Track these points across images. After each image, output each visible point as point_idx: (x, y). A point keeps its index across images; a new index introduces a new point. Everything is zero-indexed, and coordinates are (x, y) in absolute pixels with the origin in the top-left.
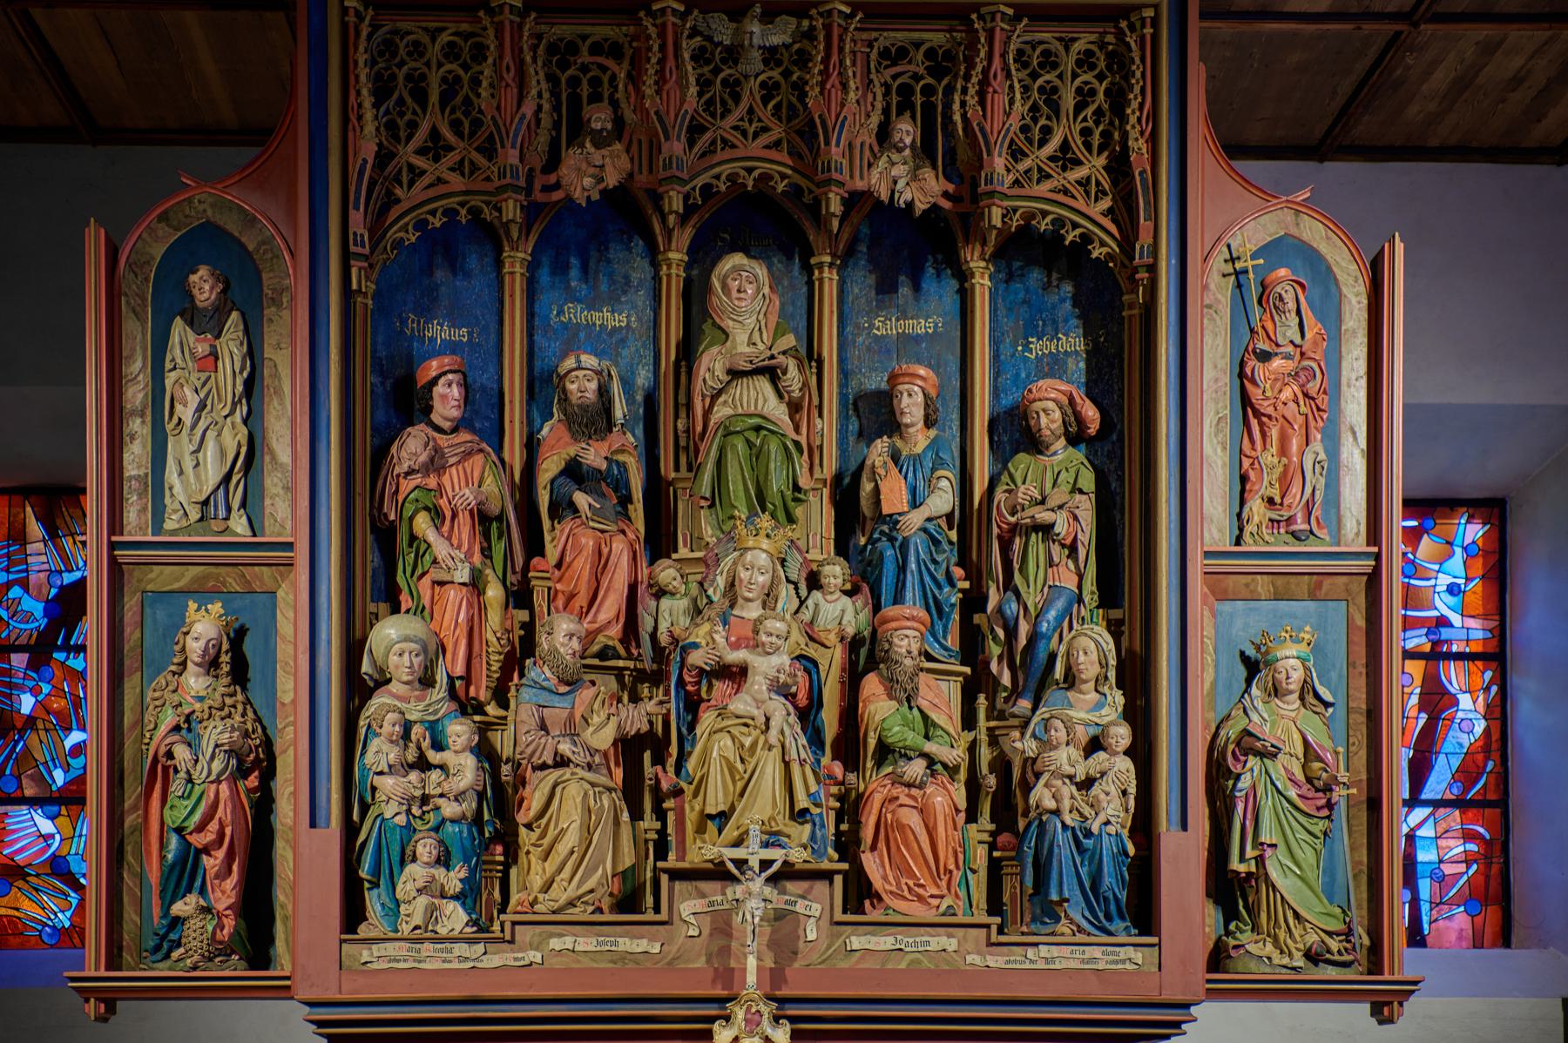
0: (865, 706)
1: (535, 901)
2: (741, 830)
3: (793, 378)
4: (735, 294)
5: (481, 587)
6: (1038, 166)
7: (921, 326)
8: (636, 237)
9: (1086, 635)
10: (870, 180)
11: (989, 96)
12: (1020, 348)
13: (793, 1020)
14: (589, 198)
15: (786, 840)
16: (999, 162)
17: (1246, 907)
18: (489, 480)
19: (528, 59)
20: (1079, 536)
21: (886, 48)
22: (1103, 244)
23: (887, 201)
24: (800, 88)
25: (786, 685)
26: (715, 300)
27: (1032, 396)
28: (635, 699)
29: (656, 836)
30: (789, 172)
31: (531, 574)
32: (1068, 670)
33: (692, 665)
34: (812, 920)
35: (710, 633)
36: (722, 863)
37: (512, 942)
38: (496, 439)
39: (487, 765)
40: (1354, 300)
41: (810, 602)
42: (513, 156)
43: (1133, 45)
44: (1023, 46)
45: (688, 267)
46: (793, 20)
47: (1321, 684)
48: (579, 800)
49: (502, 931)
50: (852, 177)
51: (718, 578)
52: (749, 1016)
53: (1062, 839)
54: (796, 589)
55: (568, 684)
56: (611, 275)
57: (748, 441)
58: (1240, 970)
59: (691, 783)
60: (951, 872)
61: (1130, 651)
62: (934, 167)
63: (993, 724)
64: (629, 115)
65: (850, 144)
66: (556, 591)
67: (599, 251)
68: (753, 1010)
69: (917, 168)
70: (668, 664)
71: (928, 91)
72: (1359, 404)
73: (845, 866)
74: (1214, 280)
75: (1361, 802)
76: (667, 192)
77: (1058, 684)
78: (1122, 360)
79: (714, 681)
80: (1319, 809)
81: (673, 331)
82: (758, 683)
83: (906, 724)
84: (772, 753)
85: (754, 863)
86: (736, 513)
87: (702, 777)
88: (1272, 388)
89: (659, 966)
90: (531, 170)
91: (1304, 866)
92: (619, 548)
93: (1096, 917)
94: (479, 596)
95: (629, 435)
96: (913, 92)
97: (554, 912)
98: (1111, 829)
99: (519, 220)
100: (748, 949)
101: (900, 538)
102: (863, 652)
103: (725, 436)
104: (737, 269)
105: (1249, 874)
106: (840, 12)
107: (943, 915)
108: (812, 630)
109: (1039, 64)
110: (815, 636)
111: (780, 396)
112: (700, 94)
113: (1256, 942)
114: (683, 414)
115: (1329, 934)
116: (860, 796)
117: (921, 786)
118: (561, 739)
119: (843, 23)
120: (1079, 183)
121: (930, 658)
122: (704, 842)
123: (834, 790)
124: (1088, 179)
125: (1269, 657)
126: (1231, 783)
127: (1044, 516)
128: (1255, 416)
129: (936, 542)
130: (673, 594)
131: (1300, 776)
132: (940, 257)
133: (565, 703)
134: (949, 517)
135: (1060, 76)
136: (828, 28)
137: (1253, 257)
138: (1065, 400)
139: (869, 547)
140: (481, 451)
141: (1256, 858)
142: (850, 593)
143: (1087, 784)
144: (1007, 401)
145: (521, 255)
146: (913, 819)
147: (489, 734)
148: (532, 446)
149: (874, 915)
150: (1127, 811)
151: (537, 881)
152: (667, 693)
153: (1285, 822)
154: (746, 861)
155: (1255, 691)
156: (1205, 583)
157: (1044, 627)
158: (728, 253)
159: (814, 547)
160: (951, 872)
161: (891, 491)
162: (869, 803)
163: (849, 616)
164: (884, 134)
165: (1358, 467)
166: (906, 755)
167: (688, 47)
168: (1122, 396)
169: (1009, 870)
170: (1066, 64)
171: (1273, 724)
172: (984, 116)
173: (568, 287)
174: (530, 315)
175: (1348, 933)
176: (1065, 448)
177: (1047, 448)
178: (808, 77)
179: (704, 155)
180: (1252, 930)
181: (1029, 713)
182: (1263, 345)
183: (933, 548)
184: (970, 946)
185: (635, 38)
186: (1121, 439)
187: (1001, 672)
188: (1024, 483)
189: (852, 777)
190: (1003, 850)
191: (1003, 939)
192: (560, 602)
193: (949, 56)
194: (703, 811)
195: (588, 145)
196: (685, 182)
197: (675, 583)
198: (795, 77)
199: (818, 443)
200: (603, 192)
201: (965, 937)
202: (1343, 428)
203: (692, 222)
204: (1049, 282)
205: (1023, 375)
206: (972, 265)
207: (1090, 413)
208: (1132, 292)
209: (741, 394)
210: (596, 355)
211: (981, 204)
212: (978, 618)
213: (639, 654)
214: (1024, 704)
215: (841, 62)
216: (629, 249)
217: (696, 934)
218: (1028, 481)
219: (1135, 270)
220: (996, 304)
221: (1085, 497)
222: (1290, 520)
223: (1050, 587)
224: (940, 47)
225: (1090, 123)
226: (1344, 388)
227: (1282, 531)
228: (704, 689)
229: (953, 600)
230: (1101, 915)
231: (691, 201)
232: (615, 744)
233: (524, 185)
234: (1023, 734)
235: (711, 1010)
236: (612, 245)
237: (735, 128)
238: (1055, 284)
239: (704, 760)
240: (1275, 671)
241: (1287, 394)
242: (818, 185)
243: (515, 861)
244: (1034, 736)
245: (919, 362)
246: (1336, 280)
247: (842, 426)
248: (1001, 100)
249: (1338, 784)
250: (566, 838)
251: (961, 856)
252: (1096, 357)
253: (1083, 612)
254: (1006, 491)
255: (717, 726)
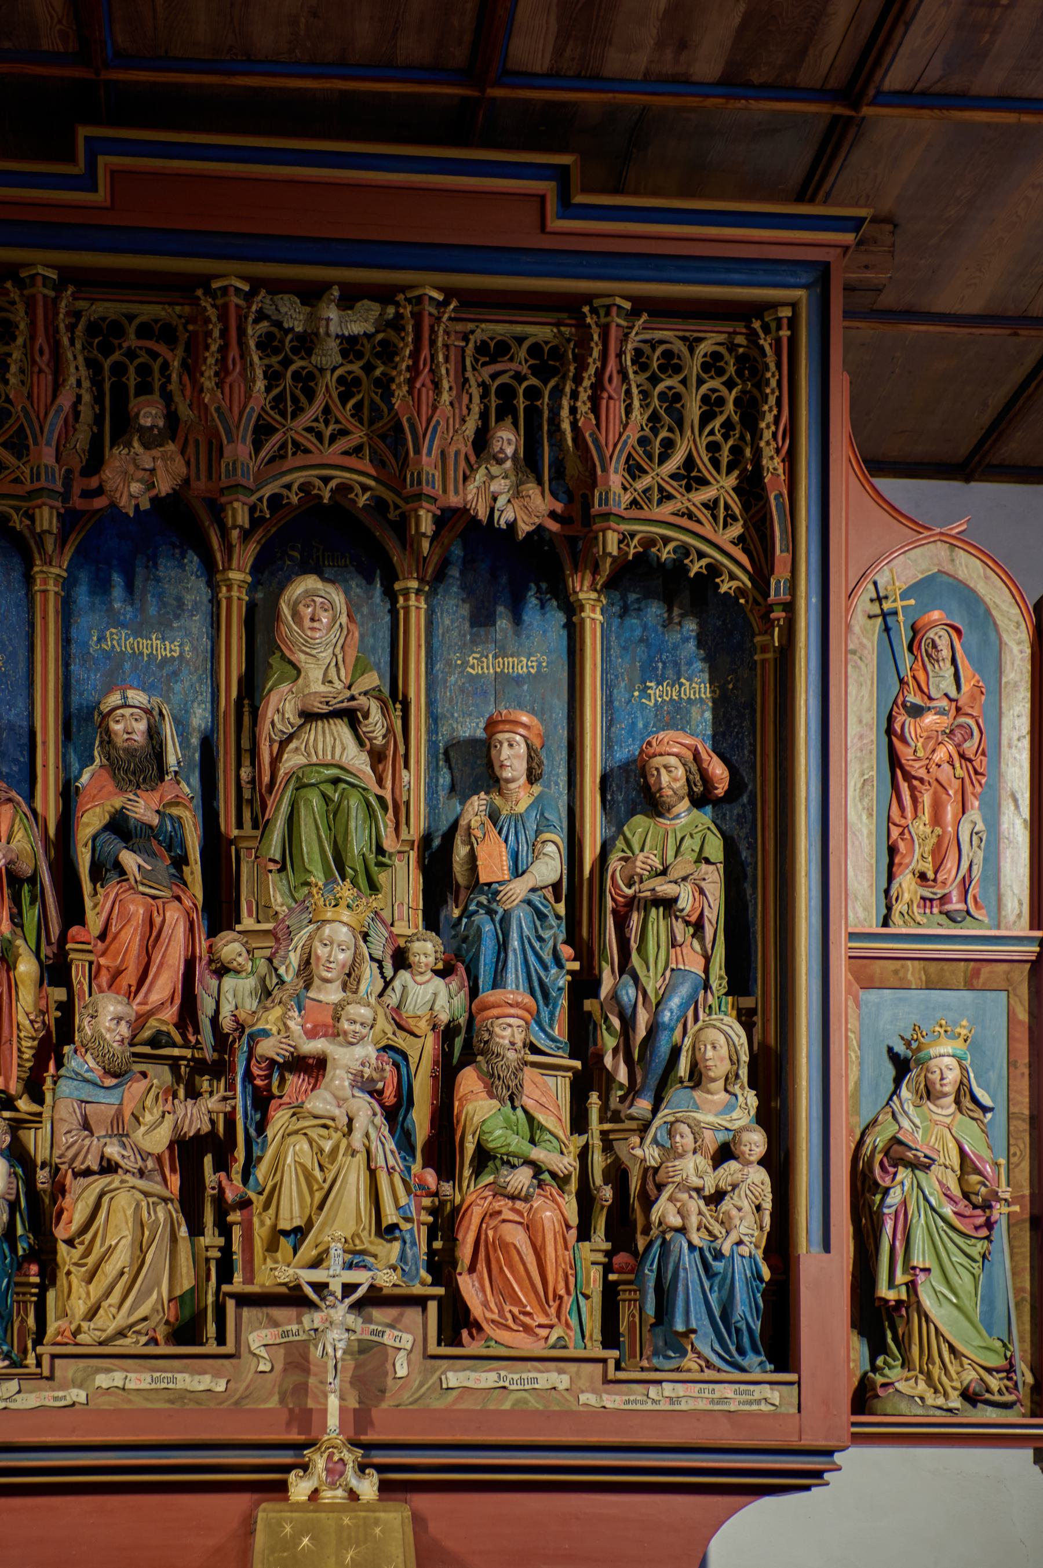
0: (462, 1106)
1: (78, 1331)
2: (320, 1249)
3: (376, 723)
4: (307, 623)
5: (11, 960)
6: (659, 486)
7: (522, 665)
8: (190, 552)
9: (714, 1027)
10: (465, 495)
11: (604, 402)
12: (636, 694)
13: (381, 1469)
14: (137, 506)
15: (371, 1260)
16: (616, 479)
17: (895, 1339)
18: (19, 835)
19: (66, 341)
20: (706, 913)
21: (483, 342)
22: (733, 577)
23: (485, 521)
24: (384, 385)
25: (371, 1080)
26: (284, 629)
27: (651, 750)
28: (193, 1094)
29: (219, 1255)
30: (372, 483)
31: (69, 946)
32: (694, 1066)
33: (261, 1056)
34: (403, 1353)
35: (283, 1019)
36: (298, 1287)
37: (51, 1378)
38: (26, 786)
39: (19, 1171)
40: (1016, 649)
41: (397, 984)
42: (48, 455)
43: (767, 348)
44: (642, 345)
45: (252, 588)
46: (376, 308)
47: (979, 1086)
48: (130, 1212)
49: (39, 1364)
50: (445, 491)
51: (292, 954)
52: (330, 1465)
53: (689, 1261)
54: (381, 967)
55: (115, 1075)
56: (160, 596)
57: (324, 795)
58: (889, 1411)
59: (260, 1193)
60: (561, 1298)
61: (764, 1046)
62: (540, 482)
63: (607, 1126)
64: (184, 411)
65: (443, 453)
66: (99, 966)
67: (147, 567)
68: (336, 1458)
69: (520, 483)
70: (232, 1053)
71: (532, 393)
72: (1021, 767)
73: (440, 1291)
74: (859, 621)
75: (1023, 1221)
76: (231, 503)
77: (682, 1082)
78: (754, 711)
79: (287, 1074)
80: (977, 1228)
81: (237, 666)
82: (338, 1078)
83: (509, 1126)
84: (356, 1160)
85: (336, 1287)
86: (313, 879)
87: (274, 1187)
88: (924, 747)
89: (224, 1406)
90: (69, 472)
91: (961, 1294)
92: (174, 919)
93: (727, 1350)
94: (8, 970)
95: (183, 785)
96: (514, 394)
97: (100, 1344)
98: (744, 1250)
99: (55, 531)
100: (329, 1388)
101: (501, 911)
102: (459, 1042)
103: (297, 789)
104: (310, 594)
105: (899, 1303)
106: (431, 298)
107: (553, 1347)
108: (400, 1015)
109: (660, 367)
110: (403, 1023)
111: (361, 743)
112: (268, 389)
113: (907, 1379)
114: (246, 761)
115: (989, 1370)
116: (456, 1209)
117: (527, 1199)
118: (108, 1140)
119: (434, 311)
120: (705, 505)
121: (535, 1050)
122: (276, 1262)
123: (427, 1202)
124: (716, 501)
125: (921, 1055)
126: (878, 1197)
127: (665, 888)
128: (905, 779)
129: (541, 916)
130: (238, 972)
131: (956, 1191)
132: (544, 586)
133: (113, 1098)
134: (556, 886)
135: (684, 382)
136: (417, 317)
137: (904, 596)
138: (689, 756)
139: (465, 920)
140: (10, 800)
141: (906, 1284)
142: (443, 973)
143: (716, 1198)
144: (622, 754)
145: (56, 571)
146: (518, 1237)
147: (21, 1133)
148: (68, 794)
149: (473, 1347)
150: (761, 1228)
151: (79, 1307)
152: (231, 1086)
153: (939, 1243)
154: (326, 1285)
155: (905, 1093)
156: (851, 970)
157: (666, 1016)
158: (298, 575)
159: (401, 919)
160: (561, 1298)
161: (490, 855)
162: (467, 1218)
163: (442, 1001)
164: (481, 442)
165: (1020, 839)
166: (508, 1162)
167: (254, 332)
168: (753, 752)
169: (627, 1296)
170: (691, 368)
171: (926, 1131)
172: (598, 425)
173: (110, 609)
174: (66, 641)
175: (1009, 1370)
176: (689, 810)
177: (669, 810)
178: (394, 373)
179: (272, 460)
180: (903, 1366)
181: (649, 1116)
182: (913, 698)
183: (538, 923)
184: (583, 1383)
185: (190, 320)
186: (752, 802)
187: (616, 1067)
188: (642, 850)
189: (447, 1188)
190: (619, 1272)
191: (621, 1375)
192: (104, 979)
193: (556, 353)
194: (275, 1225)
195: (136, 444)
196: (252, 492)
197: (240, 960)
198: (378, 373)
199: (405, 799)
200: (155, 500)
201: (578, 1373)
202: (1005, 796)
203: (257, 537)
204: (670, 619)
205: (640, 725)
206: (581, 596)
207: (718, 771)
208: (766, 633)
209: (315, 740)
210: (143, 690)
211: (595, 527)
212: (588, 1005)
213: (198, 1042)
214: (643, 1105)
215: (433, 357)
216: (182, 567)
217: (267, 1368)
218: (646, 849)
219: (770, 609)
220: (608, 642)
221: (711, 868)
222: (944, 899)
223: (673, 970)
224: (546, 343)
225: (718, 437)
226: (1004, 749)
227: (935, 910)
228: (275, 1083)
229: (561, 983)
230: (733, 1348)
231: (257, 514)
232: (170, 1147)
233: (61, 490)
234: (642, 1139)
235: (285, 1458)
236: (162, 561)
237: (309, 430)
238: (676, 620)
239: (277, 1166)
240: (928, 1070)
241: (941, 754)
242: (407, 500)
243: (53, 1283)
244: (655, 1141)
245: (520, 706)
246: (995, 624)
247: (431, 778)
248: (618, 408)
249: (999, 1200)
250: (114, 1257)
251: (572, 1279)
252: (722, 704)
253: (710, 1000)
254: (621, 859)
255: (292, 1128)
